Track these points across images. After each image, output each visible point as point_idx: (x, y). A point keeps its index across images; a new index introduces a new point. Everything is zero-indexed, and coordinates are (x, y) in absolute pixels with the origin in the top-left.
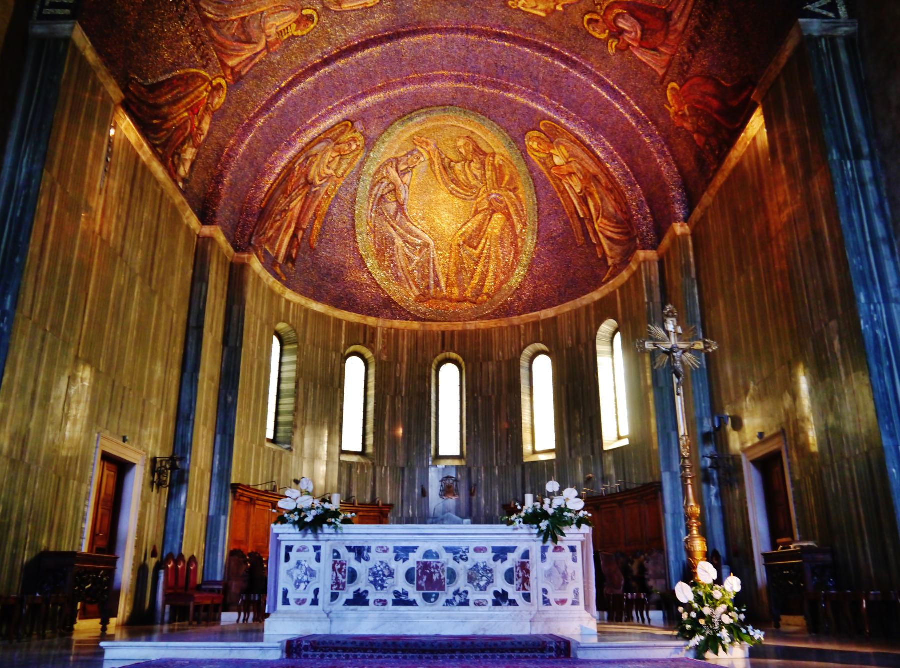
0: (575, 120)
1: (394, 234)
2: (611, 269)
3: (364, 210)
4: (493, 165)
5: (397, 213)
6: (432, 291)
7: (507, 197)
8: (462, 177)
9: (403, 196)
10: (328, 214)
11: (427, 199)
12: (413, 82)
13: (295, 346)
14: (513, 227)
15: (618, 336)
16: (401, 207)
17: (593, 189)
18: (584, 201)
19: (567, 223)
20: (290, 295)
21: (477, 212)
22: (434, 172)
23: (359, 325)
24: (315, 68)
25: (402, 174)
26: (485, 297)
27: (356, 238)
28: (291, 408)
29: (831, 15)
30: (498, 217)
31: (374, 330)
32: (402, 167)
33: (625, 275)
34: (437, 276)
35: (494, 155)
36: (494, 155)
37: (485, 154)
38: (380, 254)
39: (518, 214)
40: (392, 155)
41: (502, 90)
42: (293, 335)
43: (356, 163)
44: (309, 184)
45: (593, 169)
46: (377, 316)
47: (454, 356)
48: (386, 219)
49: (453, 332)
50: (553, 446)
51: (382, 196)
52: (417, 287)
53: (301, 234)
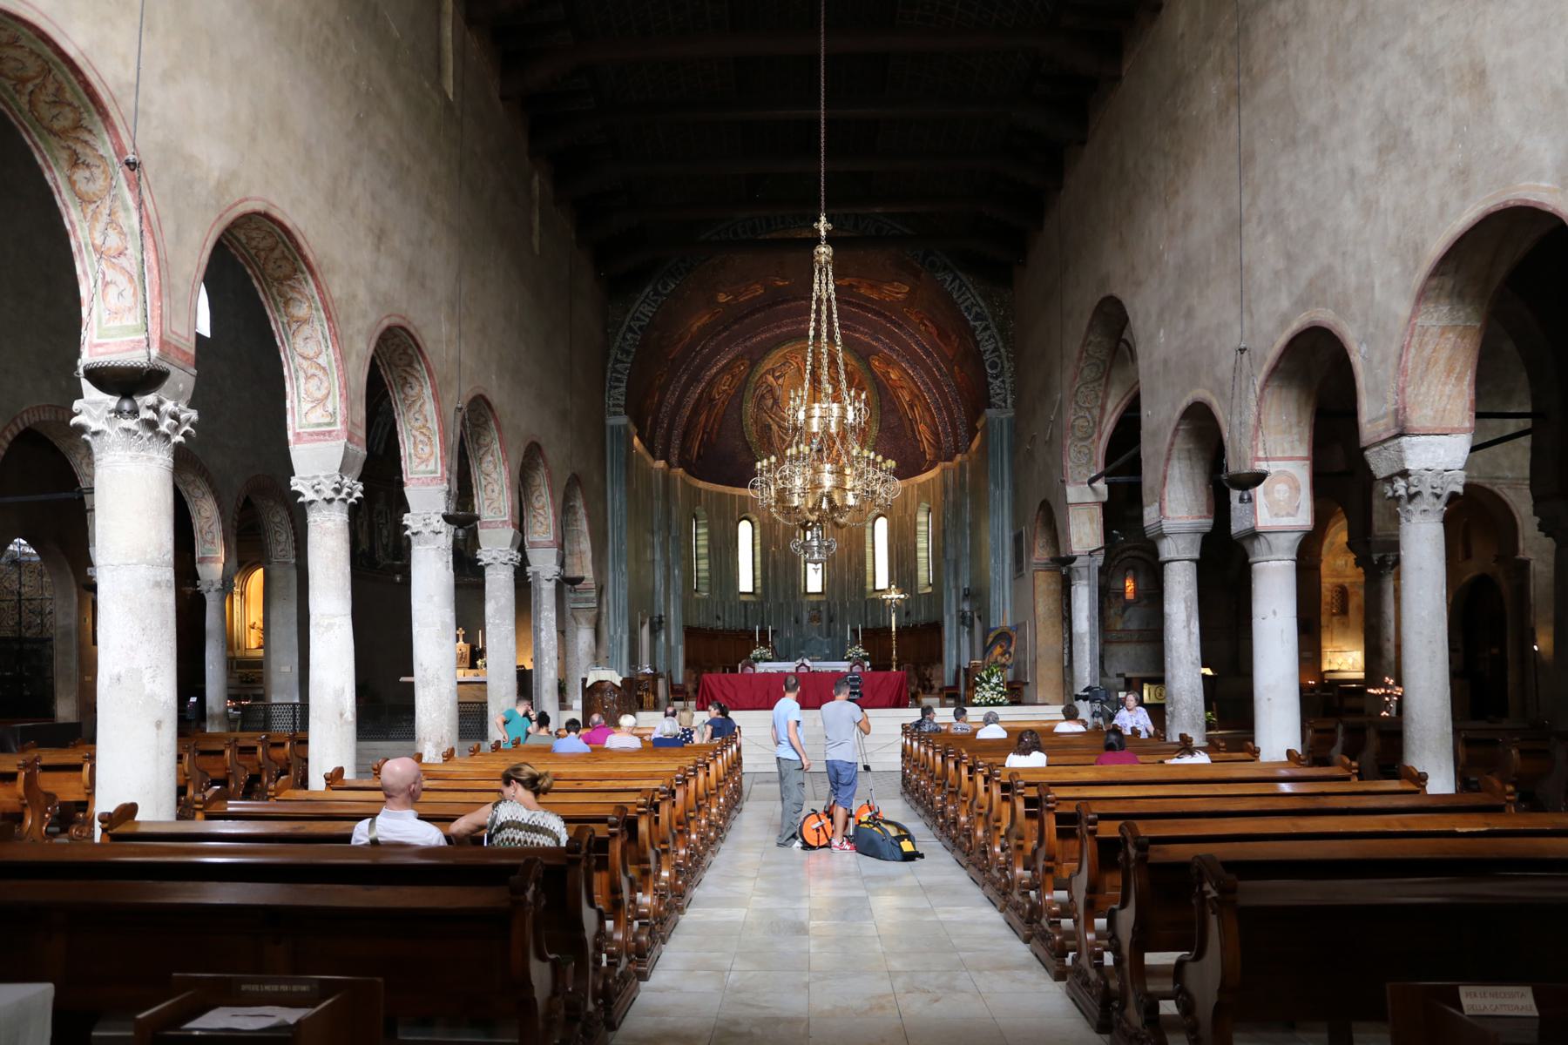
1: (772, 423)
3: (749, 408)
5: (772, 407)
10: (724, 415)
16: (776, 402)
17: (917, 402)
19: (900, 418)
24: (719, 334)
25: (779, 377)
29: (1003, 405)
40: (770, 366)
41: (851, 331)
43: (744, 377)
44: (712, 400)
45: (916, 391)
51: (762, 396)
53: (705, 436)
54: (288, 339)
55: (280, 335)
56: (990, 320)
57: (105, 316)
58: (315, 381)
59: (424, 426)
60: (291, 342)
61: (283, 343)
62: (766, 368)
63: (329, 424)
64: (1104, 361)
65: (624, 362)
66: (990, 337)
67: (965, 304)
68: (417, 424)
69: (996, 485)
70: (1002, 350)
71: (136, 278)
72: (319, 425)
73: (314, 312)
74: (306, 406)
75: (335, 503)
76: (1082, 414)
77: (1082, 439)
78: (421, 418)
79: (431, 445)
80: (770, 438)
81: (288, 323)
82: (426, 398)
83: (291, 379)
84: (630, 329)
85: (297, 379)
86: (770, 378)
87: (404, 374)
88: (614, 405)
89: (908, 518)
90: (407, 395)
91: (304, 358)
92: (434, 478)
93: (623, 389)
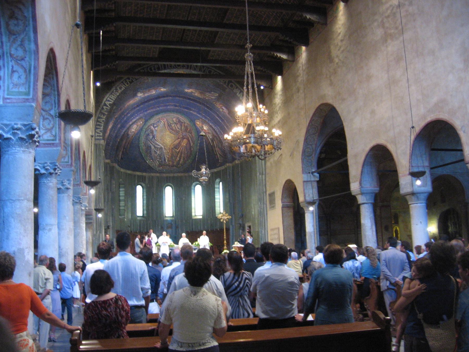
0: (210, 121)
1: (151, 145)
2: (220, 163)
3: (143, 139)
4: (184, 125)
6: (163, 162)
7: (188, 135)
8: (174, 128)
9: (155, 133)
11: (162, 134)
12: (162, 106)
13: (124, 186)
14: (190, 144)
15: (221, 183)
16: (154, 137)
17: (215, 139)
18: (212, 141)
20: (122, 170)
21: (178, 138)
22: (165, 126)
23: (141, 176)
25: (155, 127)
26: (180, 165)
27: (139, 147)
28: (124, 205)
30: (185, 140)
31: (145, 177)
32: (155, 126)
33: (223, 168)
34: (164, 158)
35: (185, 123)
36: (185, 123)
37: (182, 122)
38: (146, 151)
39: (192, 140)
41: (189, 110)
42: (123, 182)
45: (215, 135)
46: (146, 172)
47: (170, 184)
48: (149, 141)
49: (170, 177)
50: (202, 214)
52: (158, 161)
57: (11, 86)
58: (47, 121)
62: (151, 123)
63: (53, 140)
64: (317, 127)
65: (102, 118)
71: (28, 71)
72: (48, 140)
75: (54, 175)
76: (309, 147)
77: (308, 156)
79: (66, 151)
80: (150, 151)
84: (105, 105)
86: (152, 127)
88: (98, 136)
91: (44, 110)
92: (68, 165)
93: (102, 129)
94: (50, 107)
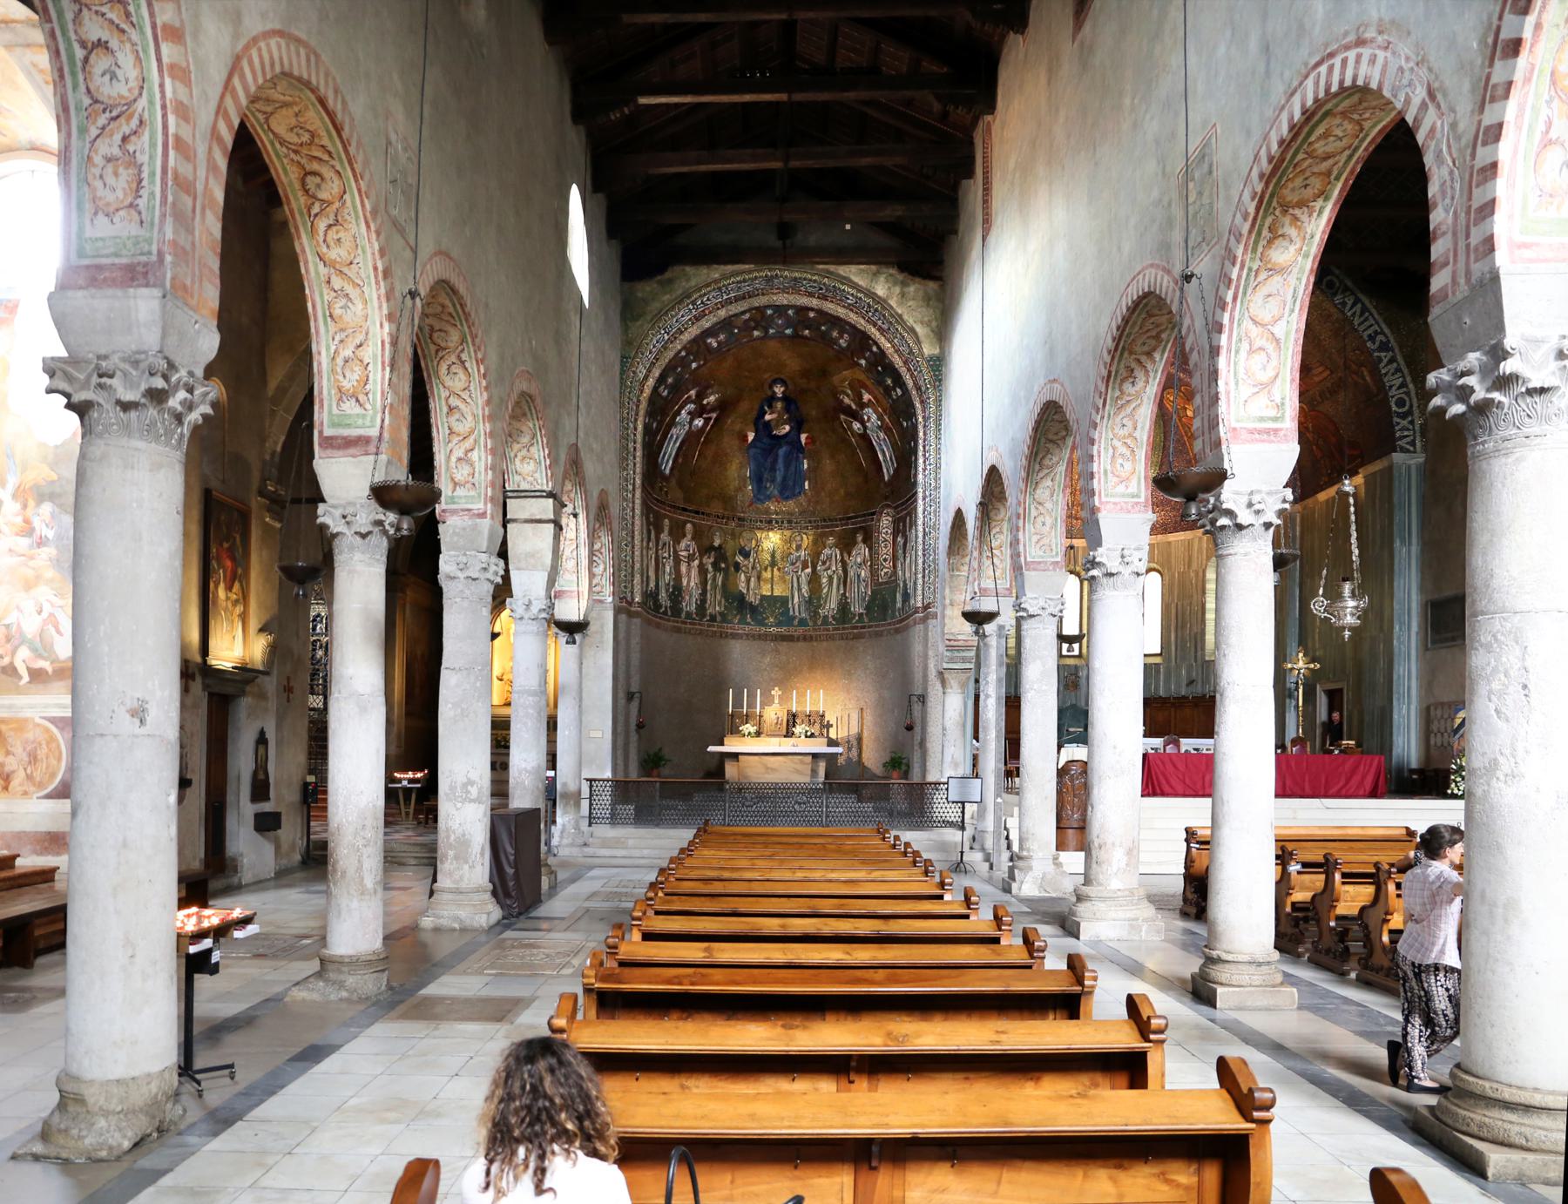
54: (1245, 293)
55: (1237, 287)
56: (1397, 350)
58: (1259, 358)
59: (1130, 435)
60: (1248, 298)
61: (1235, 298)
66: (1398, 370)
67: (1370, 331)
68: (1122, 432)
69: (1403, 541)
70: (1411, 386)
73: (1300, 259)
74: (1246, 391)
78: (1129, 424)
81: (1257, 272)
82: (1145, 399)
83: (1229, 350)
85: (1237, 352)
87: (1133, 365)
89: (1192, 575)
90: (1122, 392)
91: (1256, 323)
94: (1276, 312)
